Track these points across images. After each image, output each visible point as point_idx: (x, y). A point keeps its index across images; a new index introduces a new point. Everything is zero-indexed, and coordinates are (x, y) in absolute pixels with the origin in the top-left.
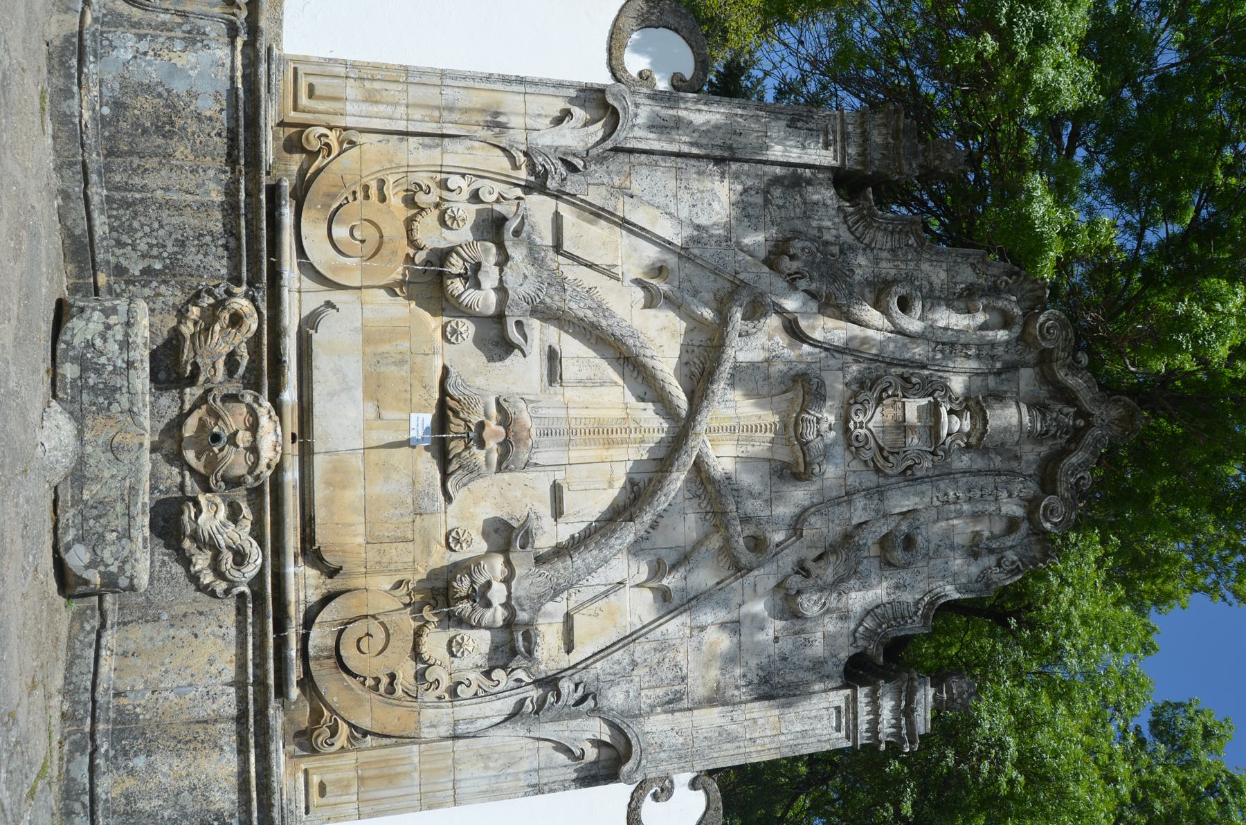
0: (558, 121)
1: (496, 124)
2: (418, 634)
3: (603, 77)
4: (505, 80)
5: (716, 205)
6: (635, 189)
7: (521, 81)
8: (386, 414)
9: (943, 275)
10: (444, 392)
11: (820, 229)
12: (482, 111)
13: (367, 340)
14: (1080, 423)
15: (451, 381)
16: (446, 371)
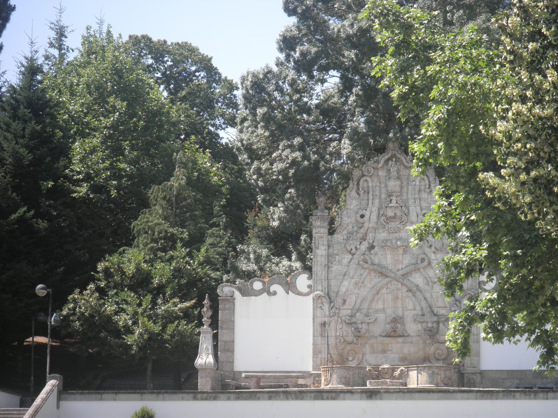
0: (322, 309)
1: (324, 324)
2: (439, 343)
3: (310, 298)
4: (314, 322)
5: (340, 269)
6: (336, 290)
7: (314, 319)
8: (390, 349)
9: (354, 201)
10: (385, 336)
11: (344, 239)
12: (321, 327)
13: (374, 353)
14: (394, 159)
15: (383, 335)
16: (380, 336)
